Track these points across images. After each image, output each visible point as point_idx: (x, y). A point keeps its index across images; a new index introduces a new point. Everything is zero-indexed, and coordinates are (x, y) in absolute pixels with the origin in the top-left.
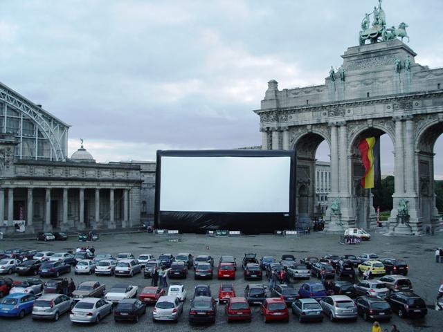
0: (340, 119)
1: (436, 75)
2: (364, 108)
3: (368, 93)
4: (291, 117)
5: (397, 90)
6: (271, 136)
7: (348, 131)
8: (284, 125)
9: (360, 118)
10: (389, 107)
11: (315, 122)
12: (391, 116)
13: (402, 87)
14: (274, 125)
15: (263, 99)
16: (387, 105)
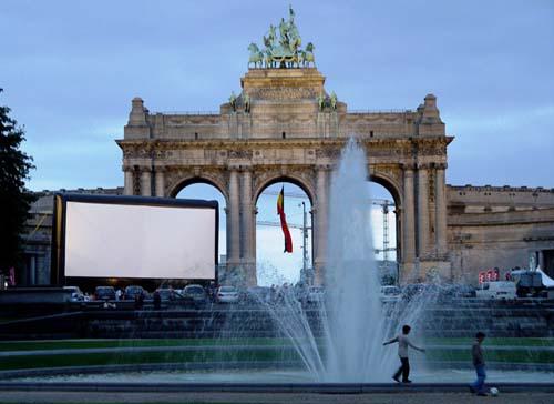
0: (245, 163)
1: (368, 120)
2: (278, 151)
3: (284, 134)
4: (170, 154)
5: (322, 132)
6: (138, 179)
7: (254, 178)
8: (158, 163)
9: (272, 163)
10: (310, 153)
11: (208, 163)
12: (313, 163)
13: (328, 131)
14: (148, 162)
15: (126, 124)
16: (308, 150)
